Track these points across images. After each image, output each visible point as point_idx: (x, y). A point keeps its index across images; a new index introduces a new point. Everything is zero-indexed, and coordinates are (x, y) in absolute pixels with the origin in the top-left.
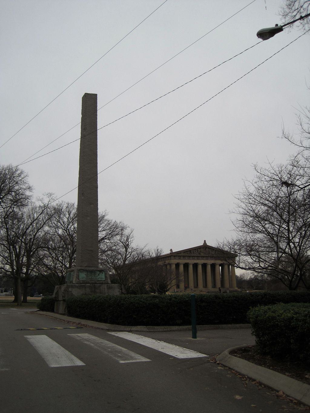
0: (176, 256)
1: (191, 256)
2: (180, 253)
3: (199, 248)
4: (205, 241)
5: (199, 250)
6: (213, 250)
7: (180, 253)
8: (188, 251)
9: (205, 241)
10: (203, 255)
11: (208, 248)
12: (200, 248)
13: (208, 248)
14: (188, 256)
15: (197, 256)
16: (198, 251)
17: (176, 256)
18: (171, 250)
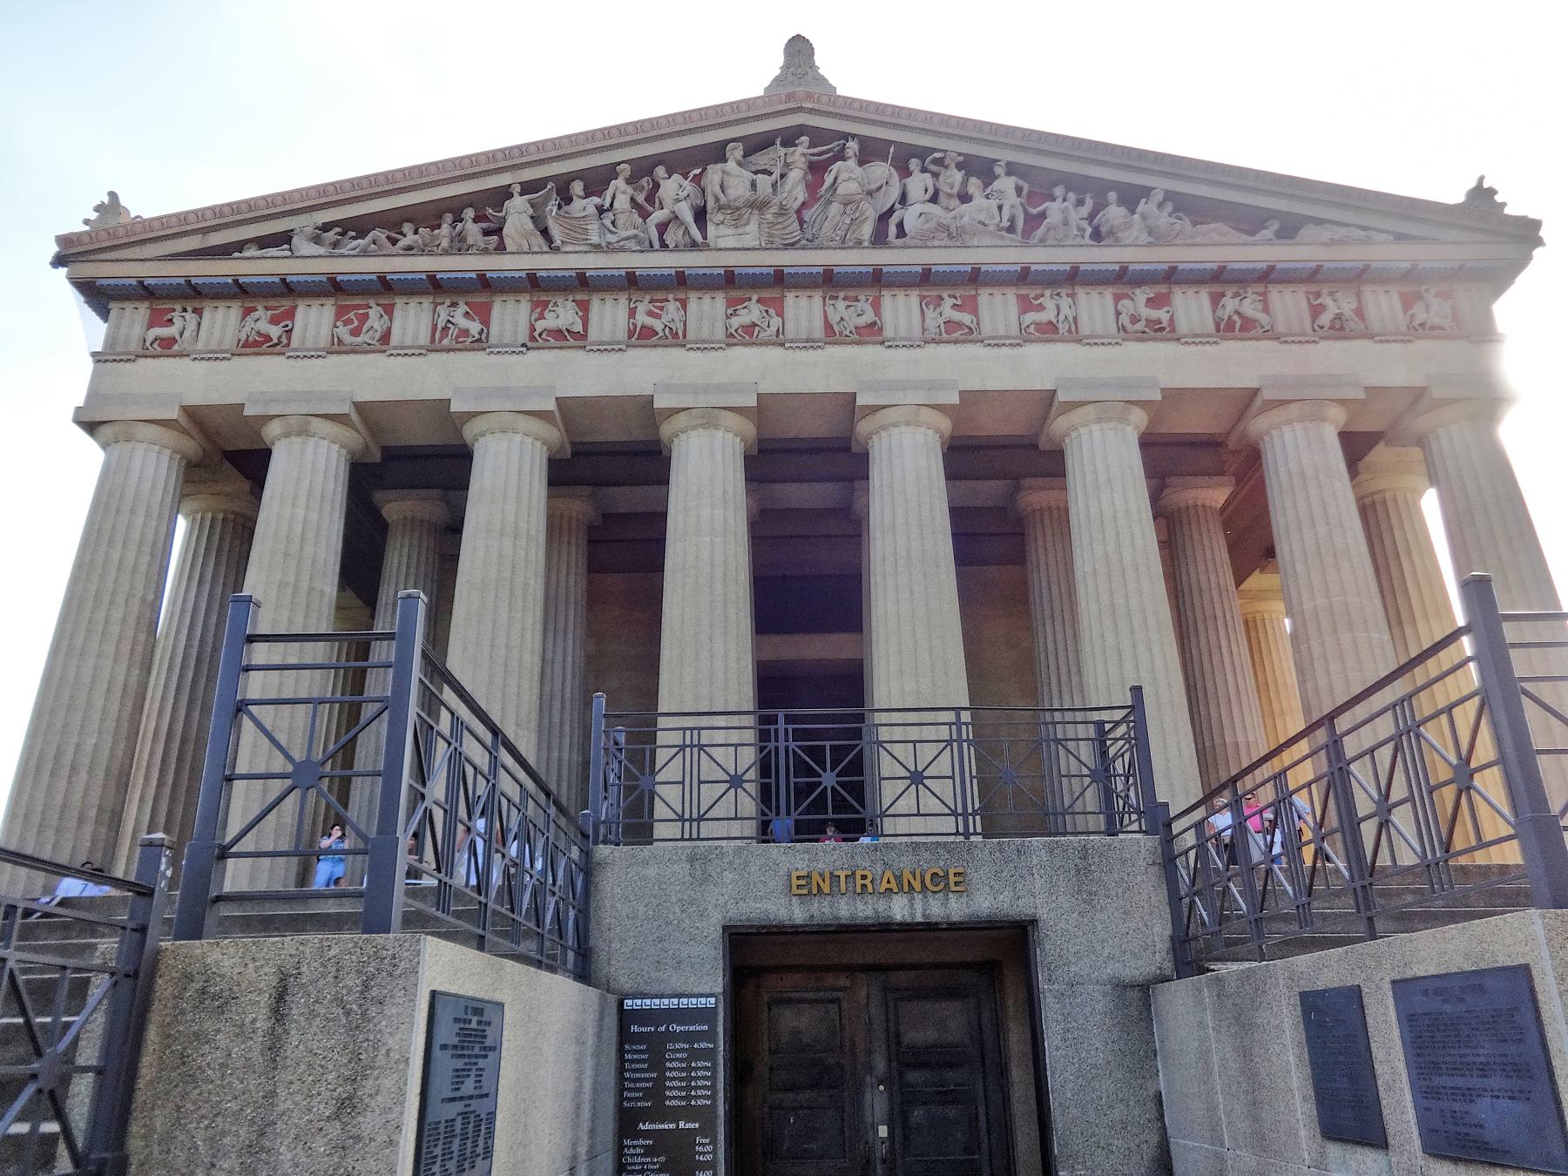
0: (194, 294)
1: (485, 284)
2: (264, 242)
3: (680, 163)
4: (799, 50)
5: (672, 187)
6: (981, 169)
7: (264, 242)
8: (455, 208)
9: (799, 50)
10: (732, 259)
11: (870, 151)
12: (717, 153)
13: (870, 151)
14: (435, 286)
15: (632, 282)
16: (645, 215)
17: (194, 294)
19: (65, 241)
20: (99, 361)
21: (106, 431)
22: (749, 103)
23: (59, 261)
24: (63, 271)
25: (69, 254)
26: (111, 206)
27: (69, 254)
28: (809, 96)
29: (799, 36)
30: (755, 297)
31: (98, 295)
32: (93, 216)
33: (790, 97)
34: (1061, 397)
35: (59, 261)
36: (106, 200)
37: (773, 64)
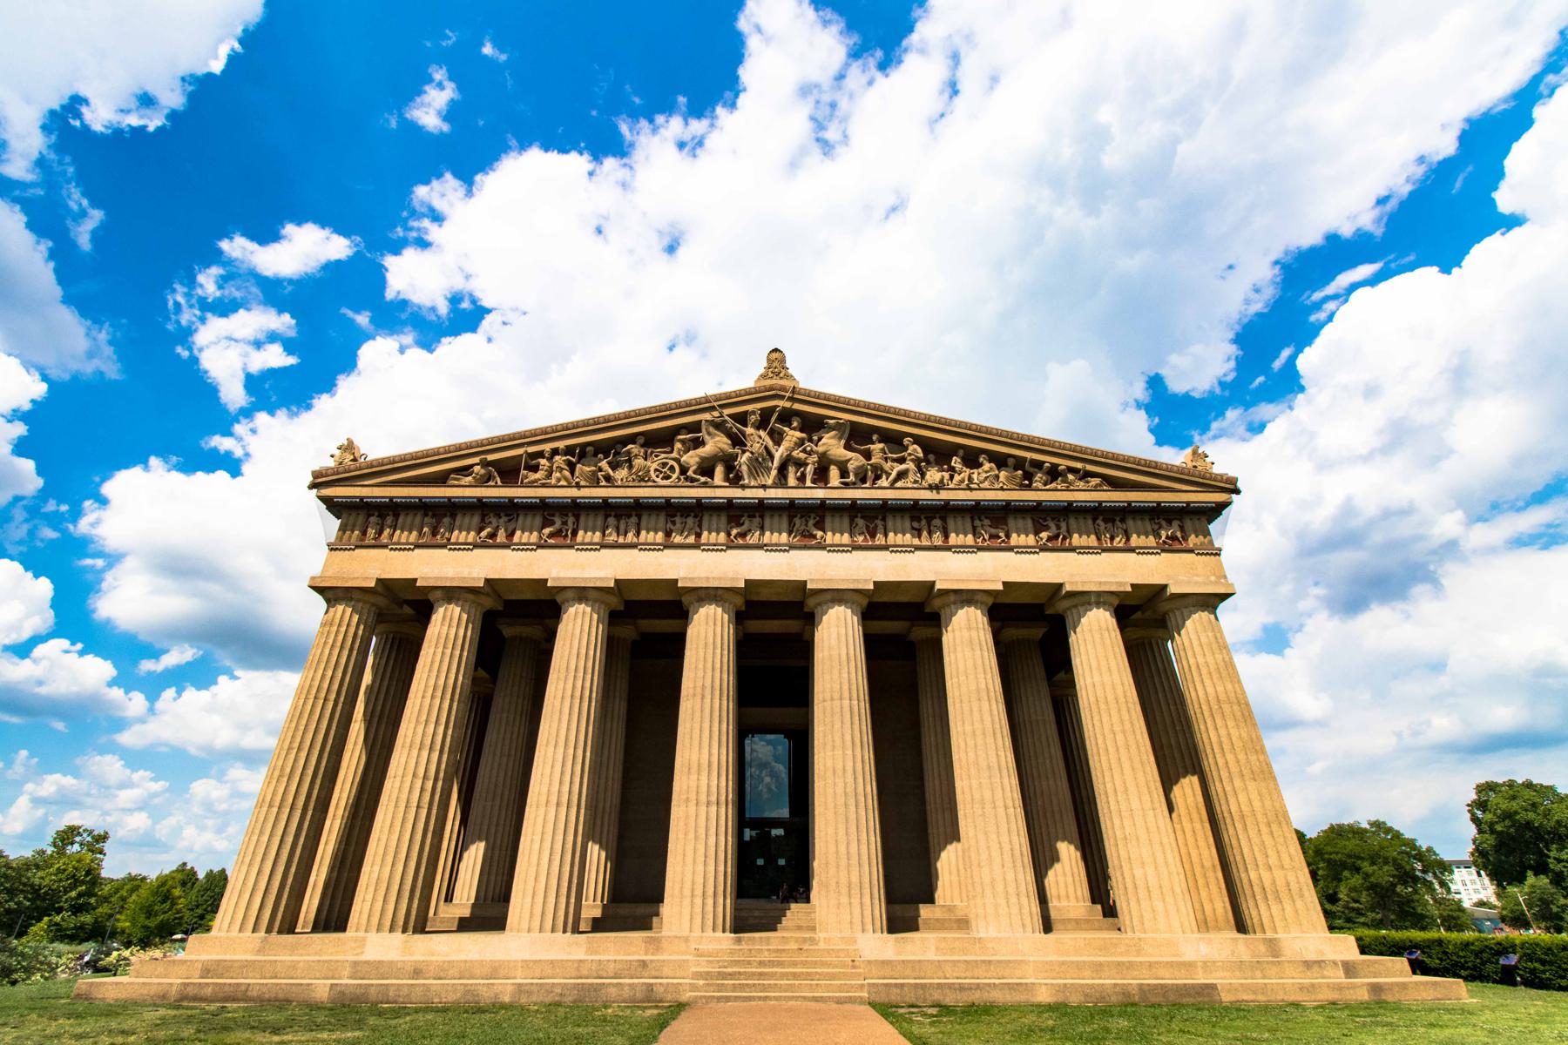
4: (776, 360)
9: (776, 360)
18: (349, 447)
19: (316, 475)
20: (332, 549)
21: (330, 594)
22: (747, 392)
23: (313, 486)
24: (315, 491)
25: (319, 481)
26: (349, 447)
27: (319, 481)
28: (784, 389)
29: (776, 350)
30: (746, 514)
31: (333, 505)
32: (337, 453)
33: (771, 389)
34: (938, 586)
35: (313, 486)
36: (346, 443)
37: (760, 366)
